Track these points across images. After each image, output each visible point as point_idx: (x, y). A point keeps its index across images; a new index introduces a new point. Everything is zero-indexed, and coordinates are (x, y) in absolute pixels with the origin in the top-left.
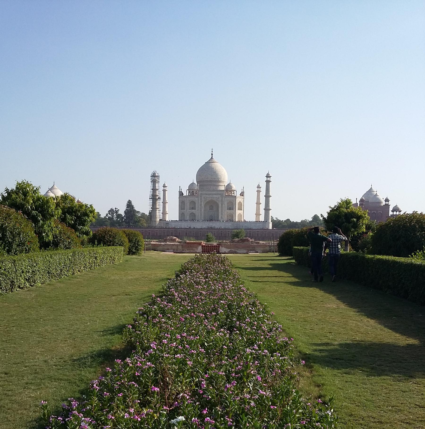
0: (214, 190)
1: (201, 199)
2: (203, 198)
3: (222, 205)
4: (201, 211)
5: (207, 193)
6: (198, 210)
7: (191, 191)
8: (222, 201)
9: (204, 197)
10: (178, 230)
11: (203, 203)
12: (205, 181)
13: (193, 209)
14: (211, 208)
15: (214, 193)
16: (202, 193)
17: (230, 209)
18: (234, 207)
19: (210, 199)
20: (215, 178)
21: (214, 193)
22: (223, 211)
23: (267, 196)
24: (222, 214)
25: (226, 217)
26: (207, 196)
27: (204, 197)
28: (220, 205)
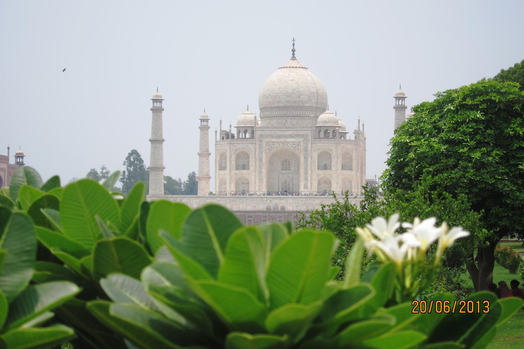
2: (264, 144)
3: (306, 158)
4: (260, 172)
7: (242, 130)
8: (306, 150)
9: (268, 143)
11: (264, 156)
13: (245, 167)
14: (286, 165)
16: (263, 133)
18: (333, 163)
20: (295, 102)
22: (309, 172)
24: (306, 179)
25: (315, 184)
26: (274, 140)
27: (268, 143)
28: (302, 160)
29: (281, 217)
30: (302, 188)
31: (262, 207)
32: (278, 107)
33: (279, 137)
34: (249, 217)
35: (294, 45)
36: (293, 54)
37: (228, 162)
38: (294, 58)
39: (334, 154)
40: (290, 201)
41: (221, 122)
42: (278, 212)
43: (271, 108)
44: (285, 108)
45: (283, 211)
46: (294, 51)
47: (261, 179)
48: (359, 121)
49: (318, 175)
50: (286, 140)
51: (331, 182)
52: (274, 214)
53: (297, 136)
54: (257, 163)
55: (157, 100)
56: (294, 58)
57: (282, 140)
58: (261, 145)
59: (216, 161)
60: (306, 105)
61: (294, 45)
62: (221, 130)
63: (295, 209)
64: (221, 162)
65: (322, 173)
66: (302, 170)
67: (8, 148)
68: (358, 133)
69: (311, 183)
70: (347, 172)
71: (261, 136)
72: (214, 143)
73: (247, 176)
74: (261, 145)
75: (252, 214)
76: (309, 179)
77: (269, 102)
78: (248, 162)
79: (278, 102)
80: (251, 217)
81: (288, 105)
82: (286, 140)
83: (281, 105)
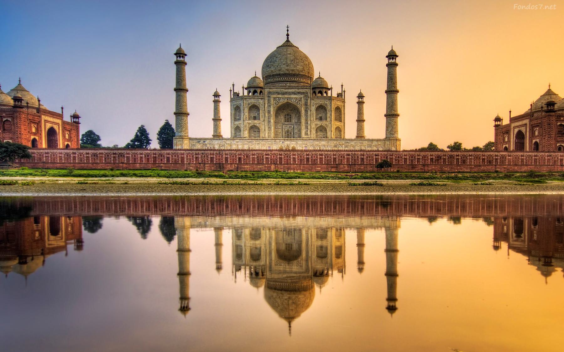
0: (290, 87)
1: (269, 102)
2: (272, 100)
3: (306, 111)
4: (269, 122)
5: (279, 90)
6: (264, 121)
7: (252, 90)
8: (306, 104)
9: (274, 98)
10: (224, 152)
11: (272, 109)
12: (277, 75)
13: (255, 118)
15: (293, 90)
16: (271, 90)
17: (321, 119)
18: (328, 115)
19: (286, 101)
20: (293, 70)
21: (293, 90)
22: (309, 122)
23: (392, 91)
24: (307, 127)
25: (314, 132)
26: (280, 96)
28: (303, 112)
29: (295, 155)
30: (303, 135)
31: (275, 147)
32: (279, 74)
34: (266, 155)
35: (288, 30)
36: (288, 38)
37: (242, 114)
38: (288, 41)
39: (328, 108)
40: (300, 142)
41: (233, 85)
42: (289, 151)
43: (273, 75)
44: (285, 75)
45: (294, 150)
46: (288, 35)
47: (269, 128)
48: (342, 86)
49: (316, 125)
50: (289, 96)
51: (326, 130)
52: (289, 153)
53: (299, 93)
54: (267, 115)
56: (288, 41)
57: (286, 96)
58: (269, 101)
59: (231, 114)
60: (301, 73)
61: (288, 30)
63: (304, 149)
64: (235, 114)
65: (319, 123)
66: (303, 121)
67: (62, 108)
70: (338, 124)
71: (269, 93)
72: (229, 100)
73: (258, 125)
74: (269, 101)
75: (269, 152)
76: (309, 127)
77: (272, 71)
78: (259, 114)
79: (279, 70)
80: (268, 155)
81: (287, 72)
82: (289, 96)
83: (282, 73)
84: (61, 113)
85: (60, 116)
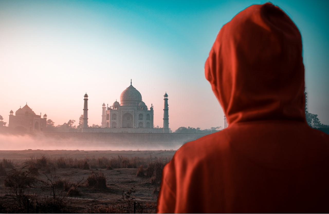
3: (135, 116)
22: (136, 121)
25: (138, 125)
30: (133, 126)
33: (126, 109)
36: (131, 84)
38: (131, 85)
46: (131, 83)
55: (86, 96)
56: (131, 85)
57: (127, 110)
61: (131, 81)
62: (108, 107)
65: (140, 121)
68: (152, 109)
69: (137, 124)
76: (136, 123)
84: (40, 115)
85: (40, 116)
